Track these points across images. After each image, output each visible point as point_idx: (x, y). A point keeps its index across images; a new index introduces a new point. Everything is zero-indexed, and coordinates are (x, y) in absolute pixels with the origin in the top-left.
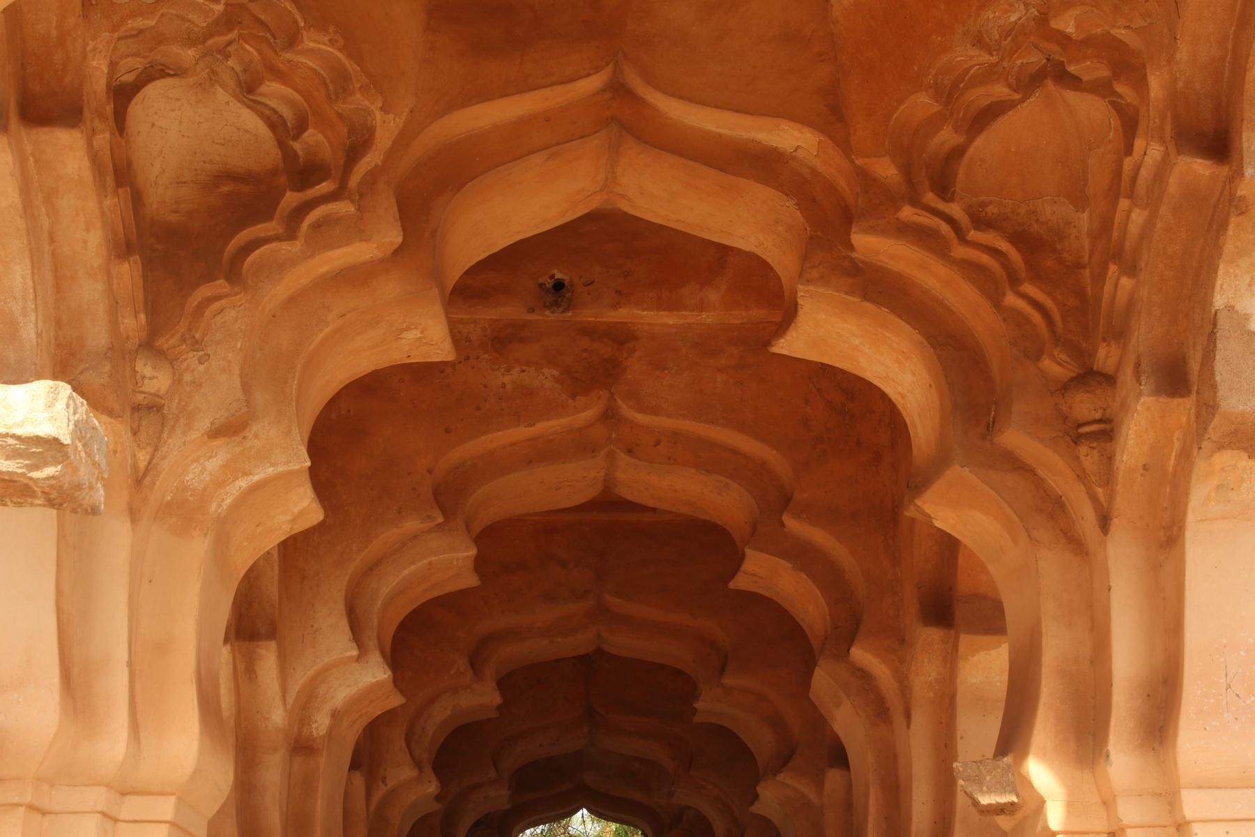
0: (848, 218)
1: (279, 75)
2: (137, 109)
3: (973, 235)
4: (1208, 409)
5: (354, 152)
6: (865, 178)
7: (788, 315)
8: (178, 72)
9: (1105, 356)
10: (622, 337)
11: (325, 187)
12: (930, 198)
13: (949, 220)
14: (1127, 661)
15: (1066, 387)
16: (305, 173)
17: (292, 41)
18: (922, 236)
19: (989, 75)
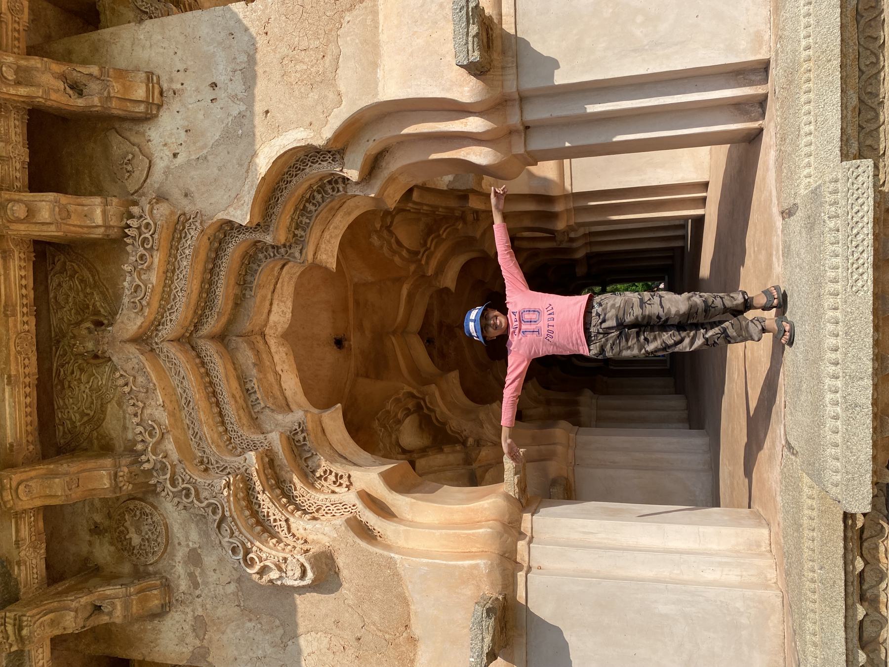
0: (423, 276)
1: (396, 415)
2: (407, 448)
3: (428, 245)
4: (473, 191)
5: (412, 396)
6: (413, 273)
7: (446, 290)
8: (397, 439)
9: (457, 213)
10: (441, 324)
11: (422, 403)
12: (419, 257)
13: (424, 252)
14: (531, 207)
15: (465, 222)
16: (419, 408)
17: (388, 412)
18: (429, 258)
19: (389, 244)
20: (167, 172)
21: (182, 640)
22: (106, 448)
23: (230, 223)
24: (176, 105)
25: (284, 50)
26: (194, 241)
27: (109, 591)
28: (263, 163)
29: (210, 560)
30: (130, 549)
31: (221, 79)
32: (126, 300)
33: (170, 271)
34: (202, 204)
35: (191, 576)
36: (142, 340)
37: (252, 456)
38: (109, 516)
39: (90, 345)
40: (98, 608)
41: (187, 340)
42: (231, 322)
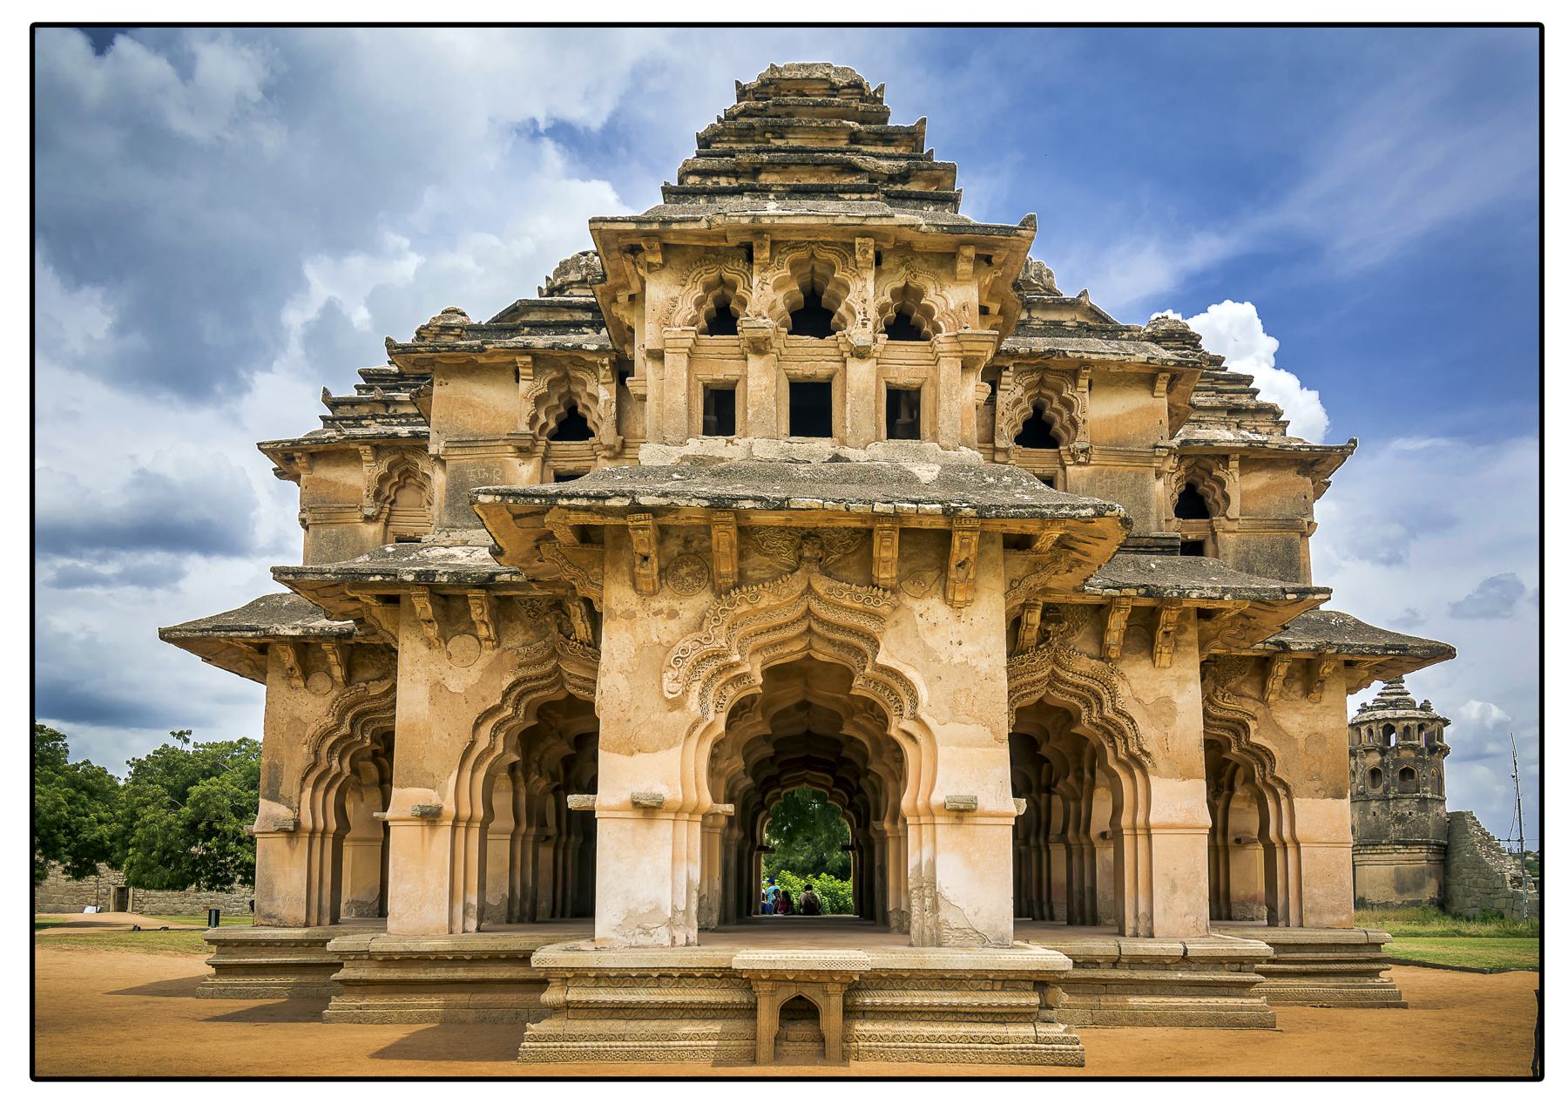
20: (911, 610)
21: (620, 602)
22: (742, 556)
23: (878, 646)
24: (952, 617)
25: (975, 689)
26: (871, 626)
27: (655, 565)
28: (911, 674)
29: (673, 624)
30: (676, 569)
31: (965, 648)
32: (834, 583)
33: (851, 610)
34: (890, 633)
35: (660, 612)
36: (809, 589)
37: (736, 658)
38: (696, 553)
39: (807, 554)
40: (646, 558)
41: (809, 611)
42: (819, 635)
